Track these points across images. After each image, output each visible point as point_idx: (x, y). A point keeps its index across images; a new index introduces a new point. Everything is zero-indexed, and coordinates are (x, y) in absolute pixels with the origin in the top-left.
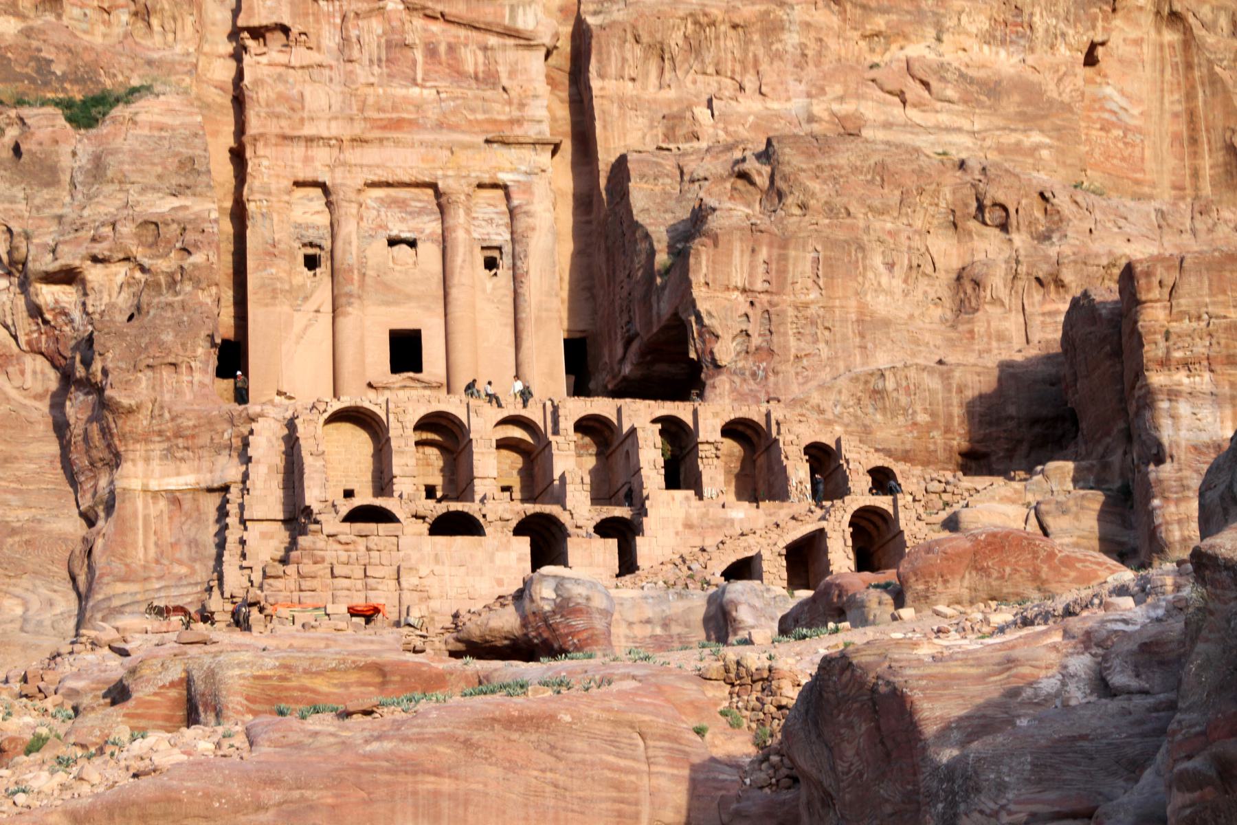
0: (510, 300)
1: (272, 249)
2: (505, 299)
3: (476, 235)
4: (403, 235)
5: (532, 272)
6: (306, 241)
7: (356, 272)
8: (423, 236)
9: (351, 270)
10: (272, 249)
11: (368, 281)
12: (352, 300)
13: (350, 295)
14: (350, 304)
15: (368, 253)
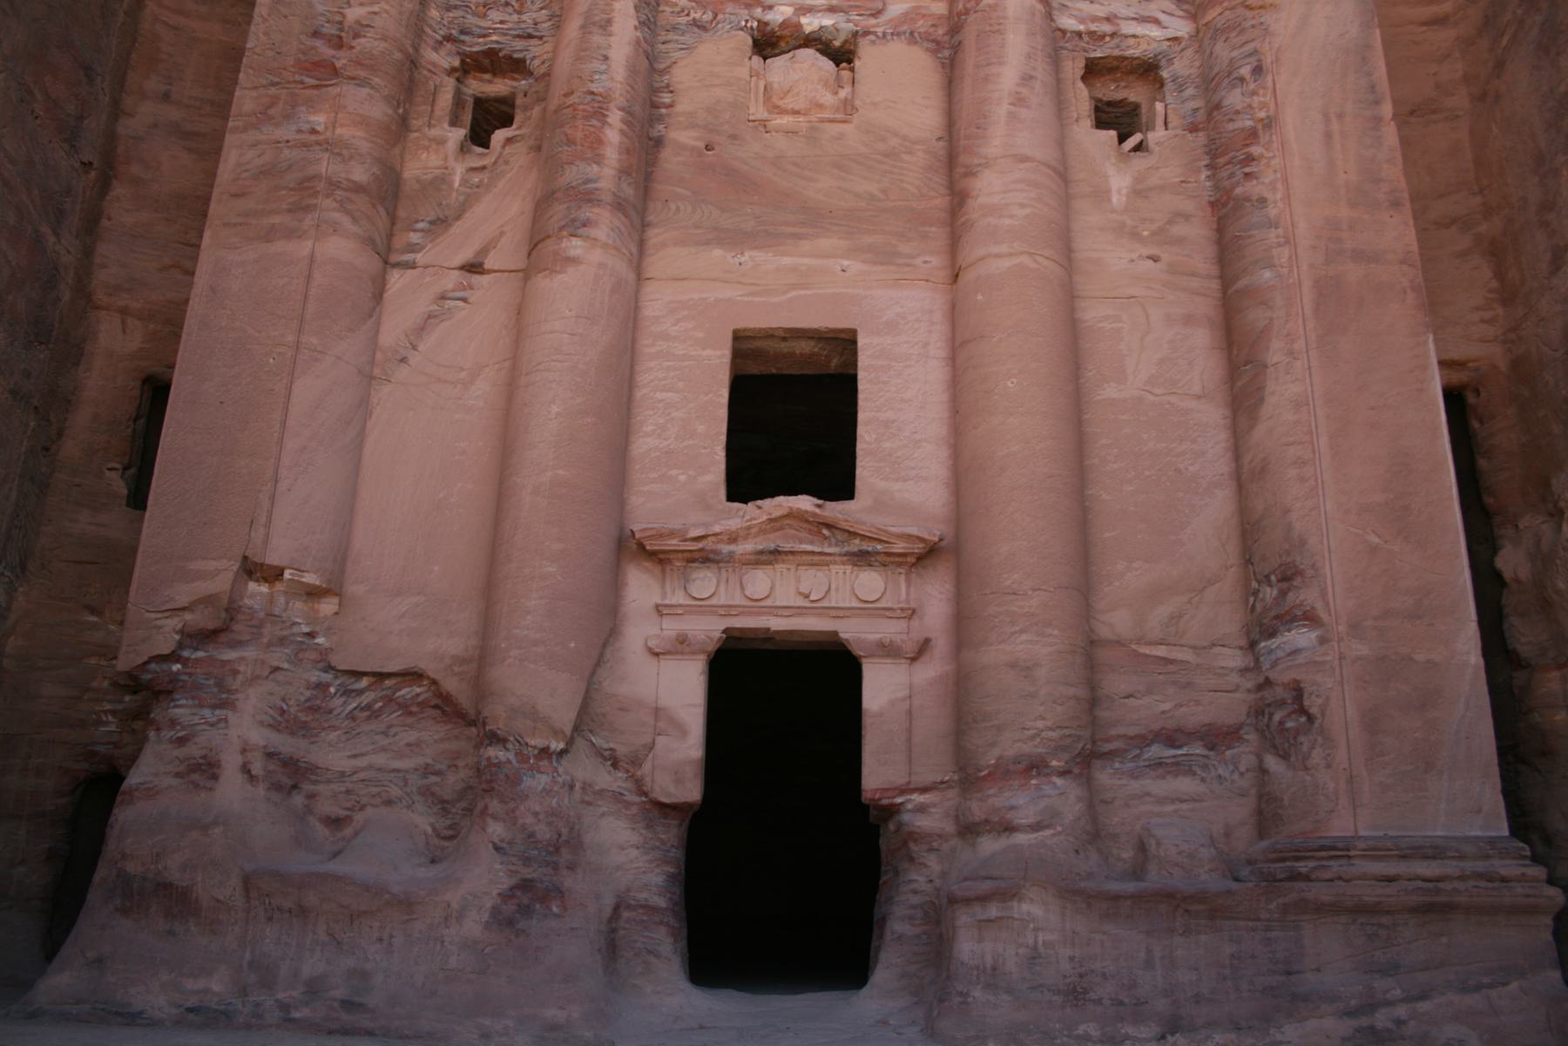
0: (1197, 231)
1: (326, 51)
2: (1180, 230)
3: (1068, 22)
4: (810, 24)
5: (1290, 119)
6: (476, 46)
7: (615, 117)
8: (879, 25)
9: (600, 114)
10: (326, 51)
11: (670, 161)
12: (587, 212)
13: (587, 196)
14: (576, 227)
15: (684, 74)
